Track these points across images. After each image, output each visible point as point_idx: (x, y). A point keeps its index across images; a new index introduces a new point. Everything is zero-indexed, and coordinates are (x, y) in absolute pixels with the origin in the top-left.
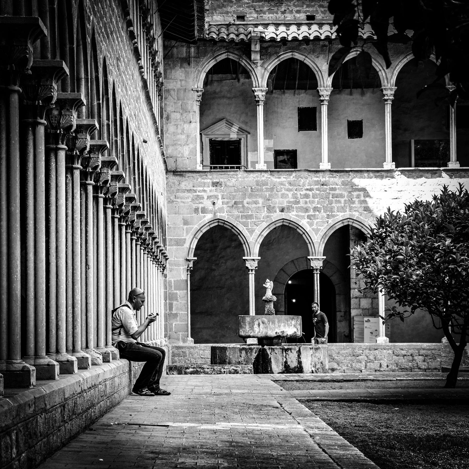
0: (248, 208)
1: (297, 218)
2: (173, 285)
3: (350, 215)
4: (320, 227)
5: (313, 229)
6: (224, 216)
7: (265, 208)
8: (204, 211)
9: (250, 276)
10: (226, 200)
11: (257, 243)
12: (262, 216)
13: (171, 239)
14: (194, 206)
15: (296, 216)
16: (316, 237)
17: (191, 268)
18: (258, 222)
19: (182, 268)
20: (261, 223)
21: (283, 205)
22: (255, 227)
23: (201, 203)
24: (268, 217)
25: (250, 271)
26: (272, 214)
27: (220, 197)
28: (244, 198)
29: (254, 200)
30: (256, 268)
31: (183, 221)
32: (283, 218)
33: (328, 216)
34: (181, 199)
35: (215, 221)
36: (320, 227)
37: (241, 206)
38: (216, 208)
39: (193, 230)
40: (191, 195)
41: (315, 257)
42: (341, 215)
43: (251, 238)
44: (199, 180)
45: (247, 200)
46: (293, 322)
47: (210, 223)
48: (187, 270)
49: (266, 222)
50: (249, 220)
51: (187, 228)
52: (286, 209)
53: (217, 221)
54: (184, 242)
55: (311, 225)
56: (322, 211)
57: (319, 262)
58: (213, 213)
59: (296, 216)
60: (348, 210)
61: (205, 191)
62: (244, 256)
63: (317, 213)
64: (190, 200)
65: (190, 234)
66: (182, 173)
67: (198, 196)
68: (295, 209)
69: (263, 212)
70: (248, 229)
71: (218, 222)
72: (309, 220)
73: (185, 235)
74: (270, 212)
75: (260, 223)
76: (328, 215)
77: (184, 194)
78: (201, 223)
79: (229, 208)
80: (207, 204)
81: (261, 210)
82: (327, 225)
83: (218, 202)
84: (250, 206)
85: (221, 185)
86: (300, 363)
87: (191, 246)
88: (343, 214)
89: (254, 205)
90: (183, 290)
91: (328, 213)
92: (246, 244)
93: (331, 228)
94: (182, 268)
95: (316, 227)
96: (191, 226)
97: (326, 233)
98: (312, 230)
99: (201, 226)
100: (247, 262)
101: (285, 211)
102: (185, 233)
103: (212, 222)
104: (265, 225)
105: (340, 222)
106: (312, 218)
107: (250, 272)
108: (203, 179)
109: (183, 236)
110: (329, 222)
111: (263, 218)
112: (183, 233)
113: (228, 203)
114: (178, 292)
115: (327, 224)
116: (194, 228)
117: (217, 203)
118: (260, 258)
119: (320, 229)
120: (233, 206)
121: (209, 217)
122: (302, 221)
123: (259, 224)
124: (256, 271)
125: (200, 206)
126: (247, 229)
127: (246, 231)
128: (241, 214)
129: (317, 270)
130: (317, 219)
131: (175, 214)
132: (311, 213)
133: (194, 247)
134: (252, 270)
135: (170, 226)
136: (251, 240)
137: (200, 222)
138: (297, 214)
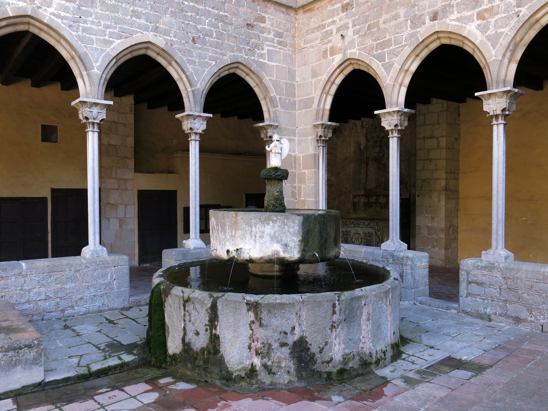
0: (385, 30)
2: (301, 162)
5: (488, 38)
6: (354, 52)
7: (409, 21)
8: (333, 52)
9: (391, 141)
10: (357, 27)
12: (404, 37)
13: (300, 100)
14: (323, 48)
15: (458, 20)
16: (493, 53)
19: (310, 138)
20: (402, 50)
21: (436, 8)
23: (330, 41)
26: (418, 30)
27: (350, 25)
28: (380, 16)
29: (393, 13)
32: (436, 30)
34: (310, 43)
35: (346, 64)
37: (375, 29)
38: (346, 43)
40: (318, 34)
43: (389, 79)
44: (328, 8)
45: (385, 17)
46: (268, 229)
48: (318, 140)
49: (410, 45)
52: (440, 14)
54: (313, 102)
55: (483, 29)
57: (498, 100)
58: (343, 51)
61: (334, 22)
64: (318, 41)
65: (318, 90)
66: (311, 7)
67: (327, 31)
70: (385, 64)
72: (480, 22)
74: (416, 27)
75: (401, 49)
77: (313, 35)
79: (360, 39)
80: (336, 39)
81: (402, 28)
82: (517, 22)
83: (348, 33)
84: (387, 26)
85: (352, 5)
86: (215, 339)
87: (322, 106)
89: (394, 22)
90: (310, 168)
94: (310, 138)
95: (494, 32)
96: (319, 78)
99: (329, 75)
101: (439, 17)
102: (313, 89)
103: (343, 66)
104: (408, 50)
106: (486, 15)
107: (390, 135)
108: (333, 5)
109: (311, 94)
111: (406, 41)
112: (312, 90)
113: (359, 30)
114: (306, 171)
115: (516, 19)
116: (323, 79)
117: (347, 34)
119: (503, 33)
120: (365, 33)
121: (338, 59)
122: (468, 27)
123: (399, 52)
125: (329, 46)
126: (383, 65)
127: (383, 70)
128: (375, 43)
129: (497, 116)
130: (497, 13)
131: (305, 65)
135: (299, 83)
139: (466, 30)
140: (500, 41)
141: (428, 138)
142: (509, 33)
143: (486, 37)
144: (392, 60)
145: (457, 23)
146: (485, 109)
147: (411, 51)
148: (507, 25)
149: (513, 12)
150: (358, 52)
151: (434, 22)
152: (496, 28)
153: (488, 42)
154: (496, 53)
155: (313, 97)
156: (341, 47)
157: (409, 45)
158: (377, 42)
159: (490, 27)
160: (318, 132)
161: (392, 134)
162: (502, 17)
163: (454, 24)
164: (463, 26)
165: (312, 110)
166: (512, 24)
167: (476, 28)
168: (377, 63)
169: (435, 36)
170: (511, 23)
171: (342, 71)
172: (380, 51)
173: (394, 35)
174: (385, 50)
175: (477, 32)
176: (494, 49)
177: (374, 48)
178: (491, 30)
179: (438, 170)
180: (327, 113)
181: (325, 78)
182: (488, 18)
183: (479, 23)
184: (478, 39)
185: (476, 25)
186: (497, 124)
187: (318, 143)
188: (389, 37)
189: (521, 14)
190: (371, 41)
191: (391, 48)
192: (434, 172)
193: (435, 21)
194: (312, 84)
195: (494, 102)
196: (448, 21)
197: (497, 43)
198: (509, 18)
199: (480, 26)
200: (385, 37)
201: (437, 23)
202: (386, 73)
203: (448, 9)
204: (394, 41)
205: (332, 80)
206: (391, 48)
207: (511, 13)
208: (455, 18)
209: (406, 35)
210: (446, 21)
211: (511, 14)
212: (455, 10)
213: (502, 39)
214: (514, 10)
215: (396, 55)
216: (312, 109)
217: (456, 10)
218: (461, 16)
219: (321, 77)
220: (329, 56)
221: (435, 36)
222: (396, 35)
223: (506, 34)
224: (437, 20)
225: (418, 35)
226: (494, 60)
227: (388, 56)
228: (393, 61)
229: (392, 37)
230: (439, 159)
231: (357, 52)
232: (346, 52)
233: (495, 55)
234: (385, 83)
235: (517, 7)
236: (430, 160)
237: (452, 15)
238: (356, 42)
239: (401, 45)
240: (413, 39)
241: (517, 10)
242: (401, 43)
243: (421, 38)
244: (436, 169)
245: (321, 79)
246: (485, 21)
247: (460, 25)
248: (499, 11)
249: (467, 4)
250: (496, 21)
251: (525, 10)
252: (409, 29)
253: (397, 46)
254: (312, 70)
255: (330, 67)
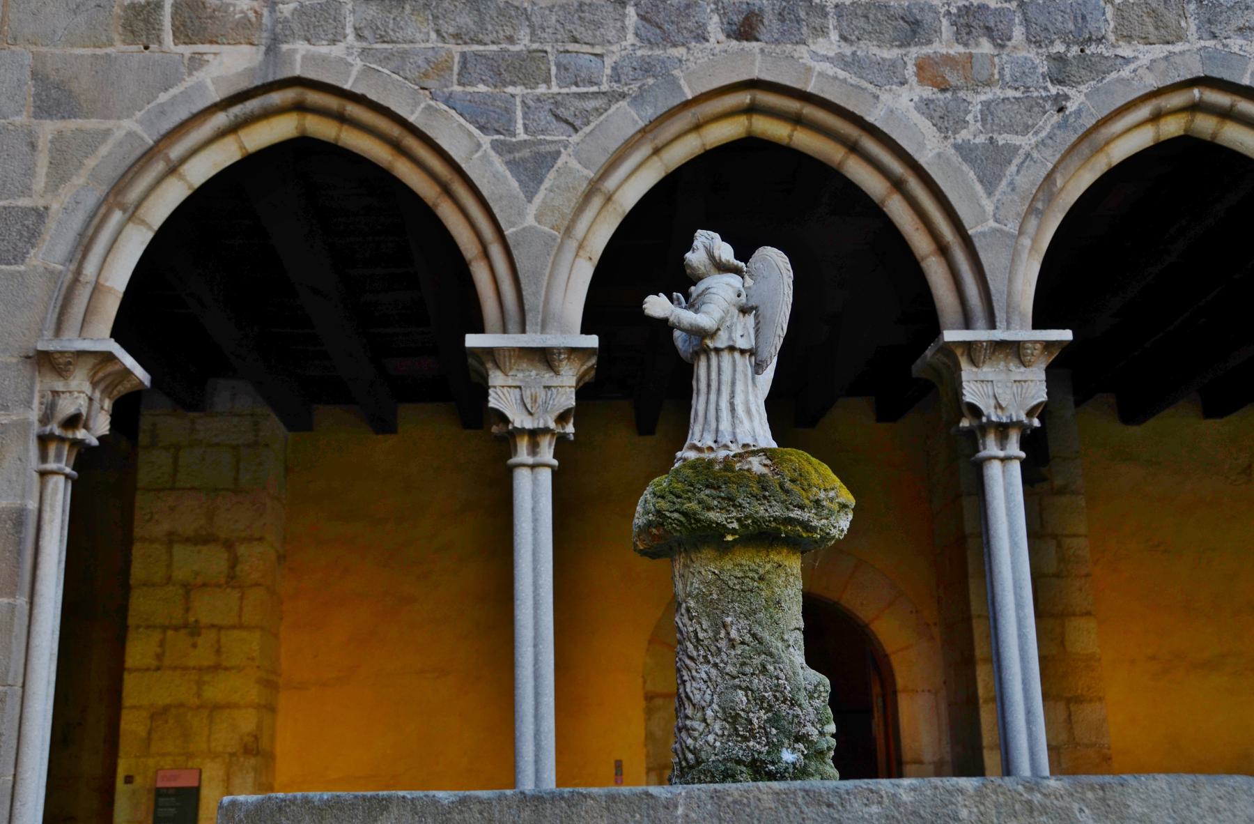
1: (853, 80)
3: (1207, 56)
4: (1016, 140)
5: (964, 150)
11: (572, 245)
12: (609, 61)
15: (841, 61)
16: (989, 207)
17: (73, 421)
18: (578, 104)
20: (599, 111)
22: (558, 134)
24: (646, 68)
25: (523, 445)
26: (680, 52)
30: (562, 418)
31: (30, 87)
32: (757, 72)
33: (1061, 72)
35: (276, 98)
36: (1016, 140)
39: (104, 150)
41: (999, 335)
42: (1144, 60)
43: (532, 210)
47: (237, 110)
49: (638, 100)
50: (518, 90)
51: (60, 132)
53: (289, 95)
54: (33, 236)
56: (1018, 33)
57: (1018, 372)
59: (841, 61)
60: (1191, 26)
62: (480, 329)
63: (986, 47)
65: (79, 180)
68: (832, 22)
69: (611, 35)
70: (512, 148)
71: (299, 107)
72: (928, 92)
73: (40, 181)
74: (668, 40)
75: (590, 104)
76: (1060, 59)
78: (173, 101)
81: (598, 25)
87: (90, 269)
88: (1159, 51)
91: (1059, 47)
92: (496, 251)
93: (1085, 148)
95: (981, 139)
96: (92, 124)
97: (1050, 177)
98: (956, 159)
99: (166, 125)
100: (496, 378)
101: (763, 32)
103: (253, 105)
105: (1145, 111)
106: (953, 78)
107: (523, 454)
109: (26, 191)
110: (1071, 107)
111: (616, 76)
112: (30, 172)
115: (1057, 118)
116: (119, 134)
118: (592, 341)
119: (1016, 149)
122: (884, 97)
124: (561, 444)
127: (498, 163)
128: (456, 49)
129: (1002, 430)
130: (988, 83)
132: (944, 45)
133: (119, 277)
134: (534, 434)
136: (530, 221)
137: (163, 97)
138: (847, 50)
139: (880, 106)
140: (1008, 173)
141: (187, 540)
142: (1035, 155)
143: (957, 147)
144: (548, 138)
145: (842, 74)
146: (969, 397)
147: (641, 124)
148: (1026, 129)
149: (1044, 94)
150: (358, 64)
151: (745, 43)
152: (988, 126)
153: (965, 167)
154: (997, 208)
155: (35, 210)
156: (251, 15)
157: (635, 99)
158: (466, 48)
159: (969, 118)
160: (56, 393)
161: (534, 448)
162: (1008, 99)
163: (831, 73)
164: (866, 89)
165: (21, 274)
166: (1042, 128)
167: (917, 108)
168: (470, 135)
169: (745, 98)
170: (1041, 123)
171: (233, 129)
172: (482, 88)
173: (557, 41)
174: (510, 89)
175: (925, 125)
176: (990, 194)
177: (451, 69)
178: (972, 128)
179: (226, 669)
180: (111, 307)
181: (131, 134)
182: (956, 89)
183: (925, 96)
184: (929, 147)
185: (916, 99)
186: (1004, 460)
187: (44, 457)
188: (535, 46)
189: (1068, 104)
190: (433, 35)
191: (542, 89)
192: (207, 678)
193: (747, 40)
194: (33, 146)
195: (1003, 377)
196: (806, 55)
197: (999, 178)
198: (1032, 107)
199: (932, 106)
200: (511, 40)
201: (757, 50)
202: (516, 184)
203: (802, 15)
204: (558, 65)
205: (176, 152)
206: (542, 89)
207: (1035, 94)
208: (831, 54)
209: (615, 58)
210: (796, 55)
211: (1037, 97)
212: (831, 27)
213: (1013, 168)
214: (1046, 89)
215: (566, 122)
216: (22, 268)
217: (835, 28)
218: (854, 53)
219: (108, 124)
220: (168, 37)
221: (745, 98)
222: (572, 47)
223: (1028, 155)
224: (757, 40)
225: (676, 72)
226: (995, 230)
227: (524, 118)
228: (553, 142)
229: (549, 49)
230: (233, 627)
231: (350, 59)
232: (285, 47)
233: (994, 215)
234: (513, 224)
235: (1052, 81)
236: (194, 630)
237: (820, 40)
238: (350, 21)
239: (595, 89)
240: (651, 81)
241: (1054, 90)
242: (592, 83)
243: (692, 92)
244: (216, 668)
245: (107, 133)
246: (948, 95)
247: (853, 82)
248: (993, 75)
249: (879, 22)
250: (987, 105)
251: (1083, 98)
252: (631, 38)
253: (574, 89)
254: (34, 75)
255: (174, 91)
